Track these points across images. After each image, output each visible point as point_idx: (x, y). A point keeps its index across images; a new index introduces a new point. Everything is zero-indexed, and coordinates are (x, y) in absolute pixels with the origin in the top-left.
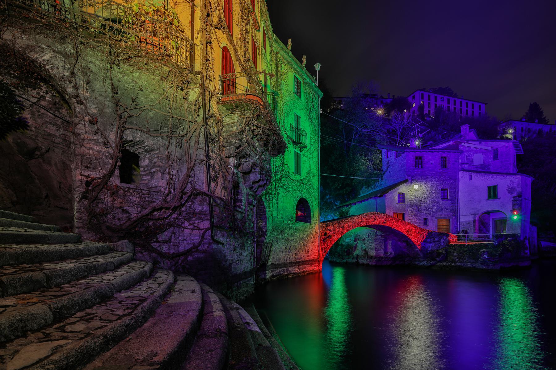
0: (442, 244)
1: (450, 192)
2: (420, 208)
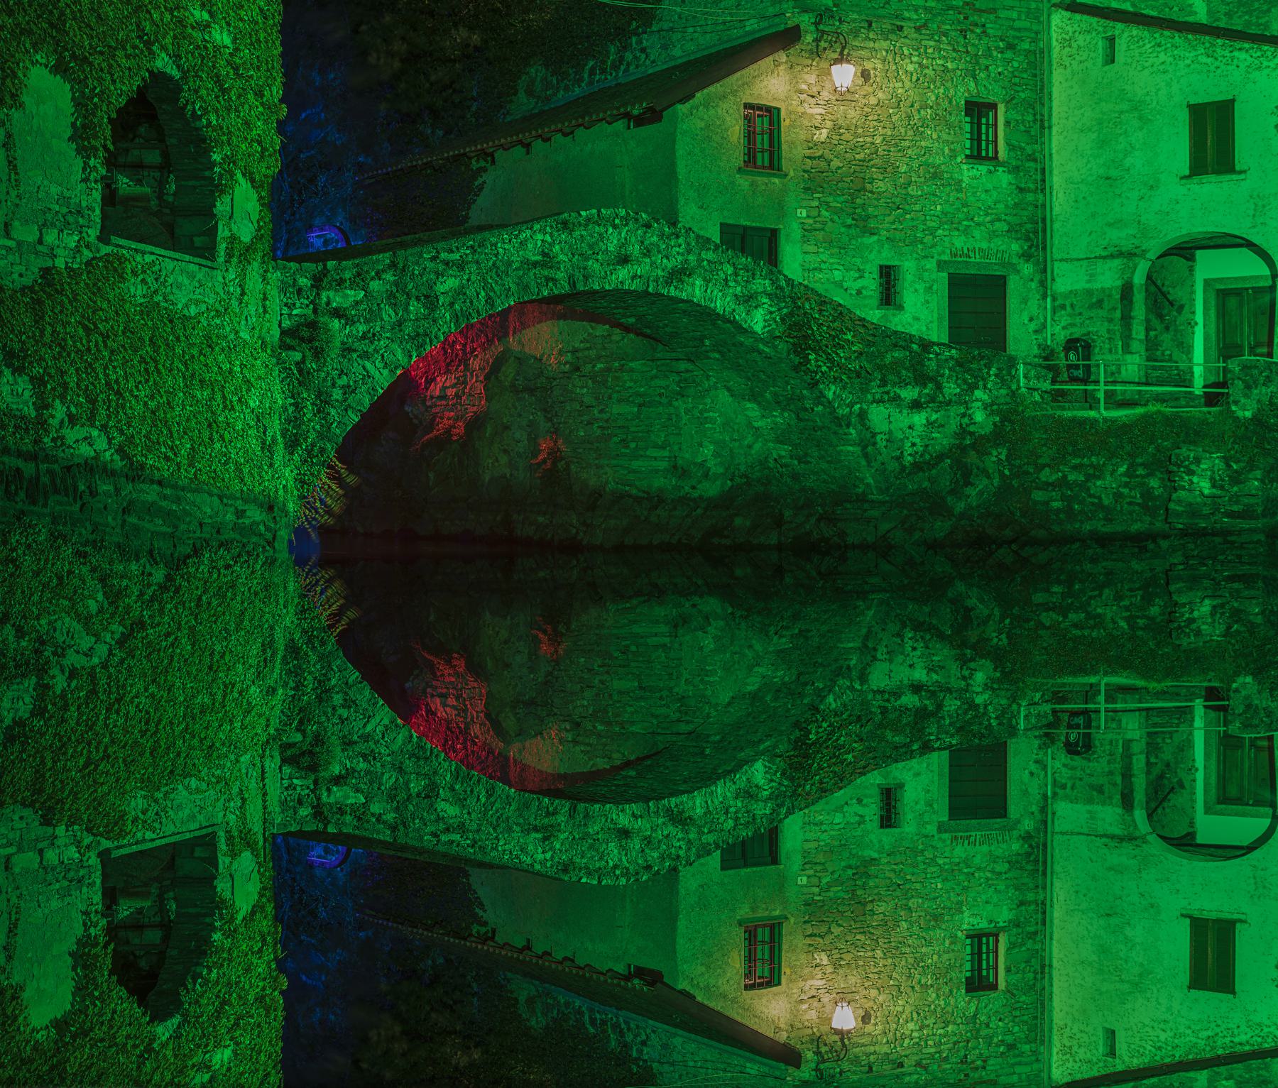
0: (979, 416)
1: (1007, 123)
2: (863, 206)
